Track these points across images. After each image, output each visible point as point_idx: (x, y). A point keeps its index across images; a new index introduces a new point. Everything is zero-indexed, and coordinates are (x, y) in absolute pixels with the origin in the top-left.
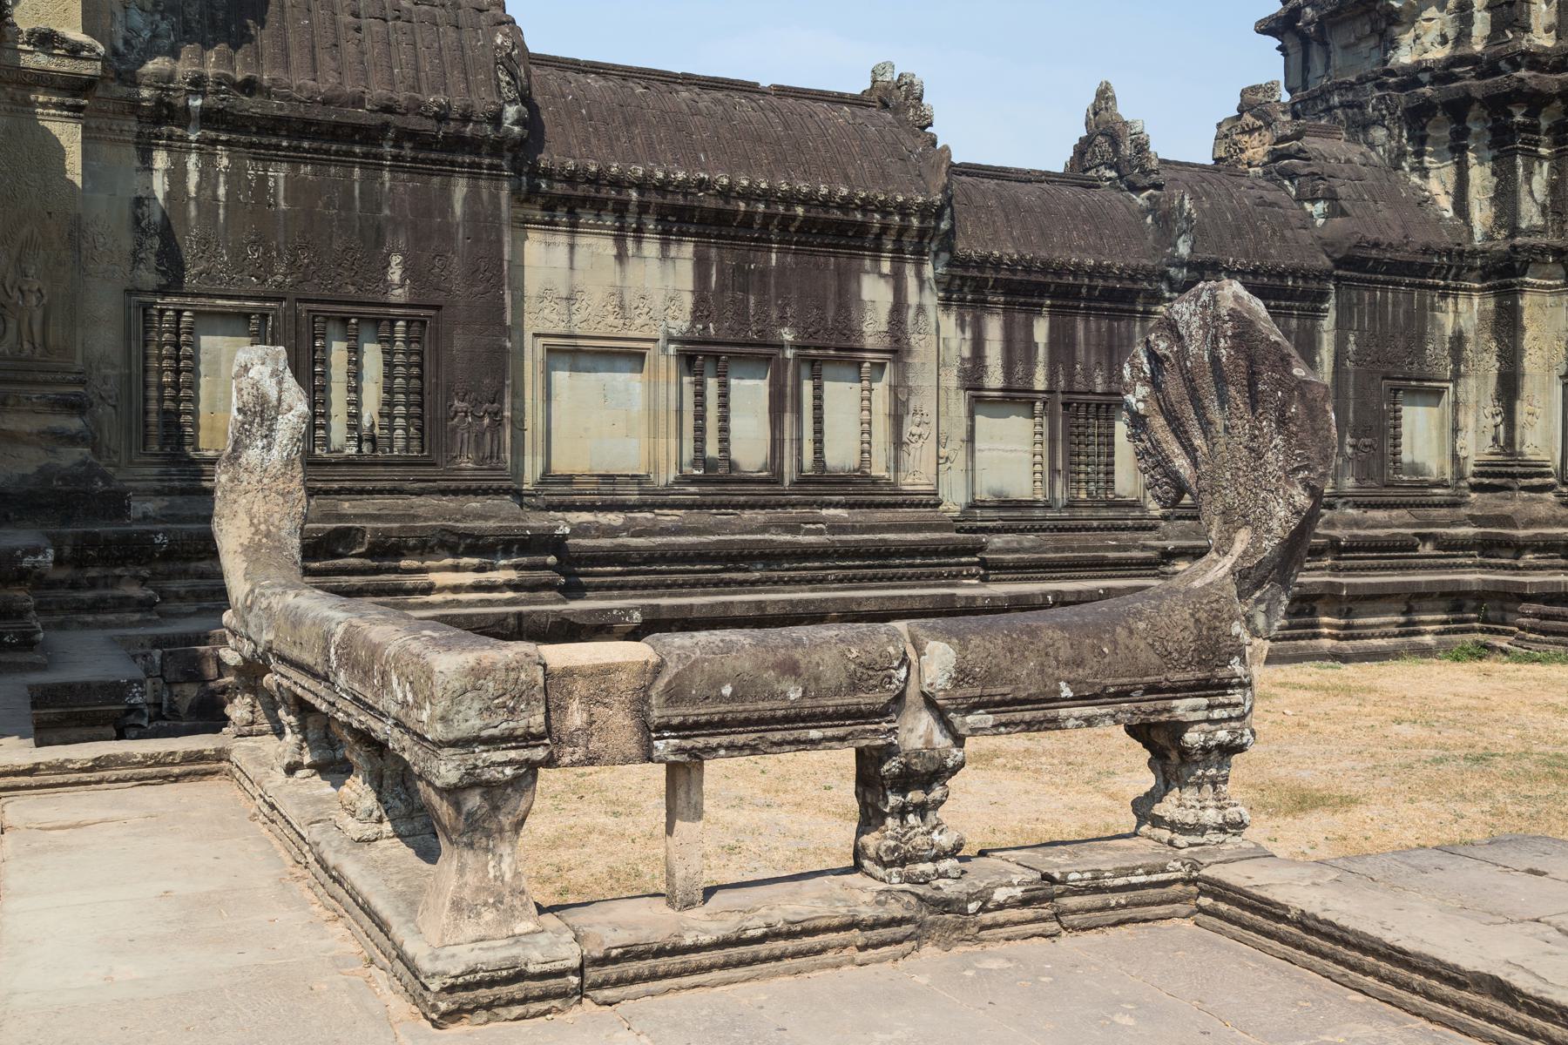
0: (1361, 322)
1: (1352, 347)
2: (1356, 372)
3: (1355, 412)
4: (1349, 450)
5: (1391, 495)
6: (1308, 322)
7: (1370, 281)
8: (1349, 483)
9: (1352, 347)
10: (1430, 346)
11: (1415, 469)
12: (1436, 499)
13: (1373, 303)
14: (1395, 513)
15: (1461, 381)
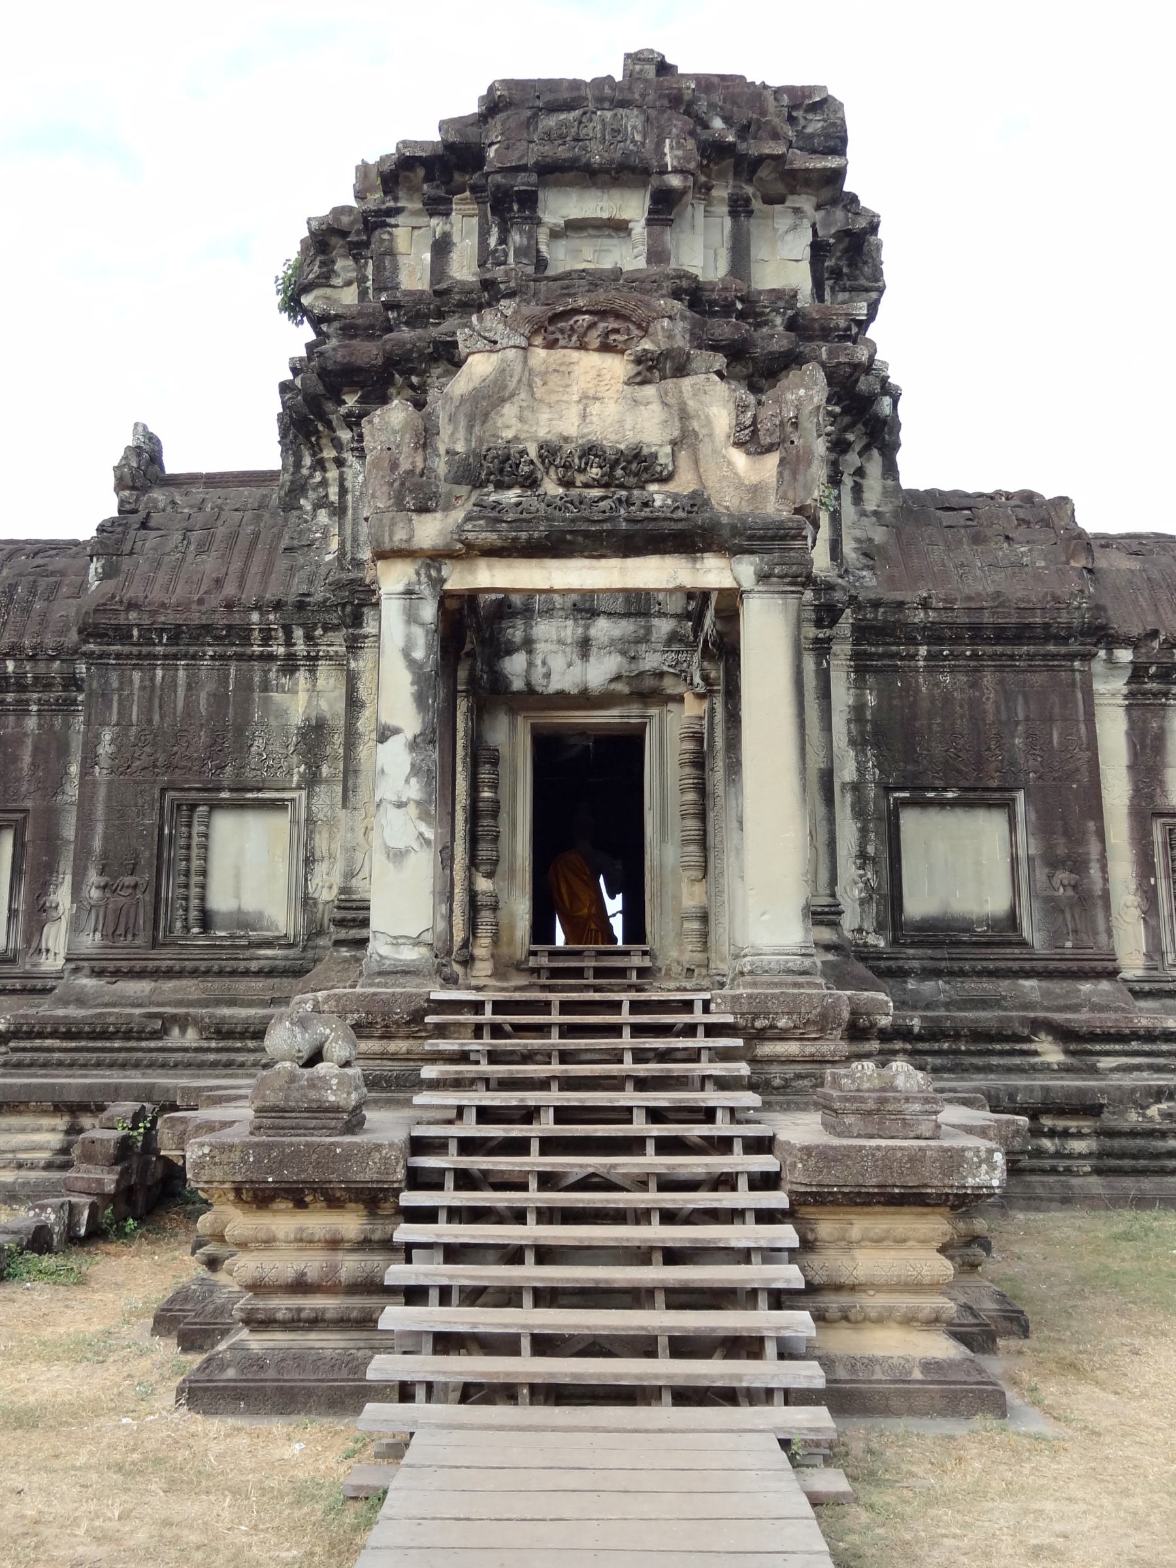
0: (124, 712)
1: (105, 748)
2: (110, 783)
3: (106, 838)
4: (95, 894)
5: (165, 957)
6: (58, 721)
7: (139, 656)
8: (90, 942)
9: (105, 748)
10: (259, 742)
11: (243, 921)
12: (254, 966)
13: (149, 688)
14: (169, 985)
15: (321, 789)
